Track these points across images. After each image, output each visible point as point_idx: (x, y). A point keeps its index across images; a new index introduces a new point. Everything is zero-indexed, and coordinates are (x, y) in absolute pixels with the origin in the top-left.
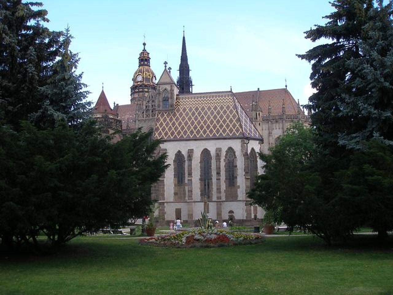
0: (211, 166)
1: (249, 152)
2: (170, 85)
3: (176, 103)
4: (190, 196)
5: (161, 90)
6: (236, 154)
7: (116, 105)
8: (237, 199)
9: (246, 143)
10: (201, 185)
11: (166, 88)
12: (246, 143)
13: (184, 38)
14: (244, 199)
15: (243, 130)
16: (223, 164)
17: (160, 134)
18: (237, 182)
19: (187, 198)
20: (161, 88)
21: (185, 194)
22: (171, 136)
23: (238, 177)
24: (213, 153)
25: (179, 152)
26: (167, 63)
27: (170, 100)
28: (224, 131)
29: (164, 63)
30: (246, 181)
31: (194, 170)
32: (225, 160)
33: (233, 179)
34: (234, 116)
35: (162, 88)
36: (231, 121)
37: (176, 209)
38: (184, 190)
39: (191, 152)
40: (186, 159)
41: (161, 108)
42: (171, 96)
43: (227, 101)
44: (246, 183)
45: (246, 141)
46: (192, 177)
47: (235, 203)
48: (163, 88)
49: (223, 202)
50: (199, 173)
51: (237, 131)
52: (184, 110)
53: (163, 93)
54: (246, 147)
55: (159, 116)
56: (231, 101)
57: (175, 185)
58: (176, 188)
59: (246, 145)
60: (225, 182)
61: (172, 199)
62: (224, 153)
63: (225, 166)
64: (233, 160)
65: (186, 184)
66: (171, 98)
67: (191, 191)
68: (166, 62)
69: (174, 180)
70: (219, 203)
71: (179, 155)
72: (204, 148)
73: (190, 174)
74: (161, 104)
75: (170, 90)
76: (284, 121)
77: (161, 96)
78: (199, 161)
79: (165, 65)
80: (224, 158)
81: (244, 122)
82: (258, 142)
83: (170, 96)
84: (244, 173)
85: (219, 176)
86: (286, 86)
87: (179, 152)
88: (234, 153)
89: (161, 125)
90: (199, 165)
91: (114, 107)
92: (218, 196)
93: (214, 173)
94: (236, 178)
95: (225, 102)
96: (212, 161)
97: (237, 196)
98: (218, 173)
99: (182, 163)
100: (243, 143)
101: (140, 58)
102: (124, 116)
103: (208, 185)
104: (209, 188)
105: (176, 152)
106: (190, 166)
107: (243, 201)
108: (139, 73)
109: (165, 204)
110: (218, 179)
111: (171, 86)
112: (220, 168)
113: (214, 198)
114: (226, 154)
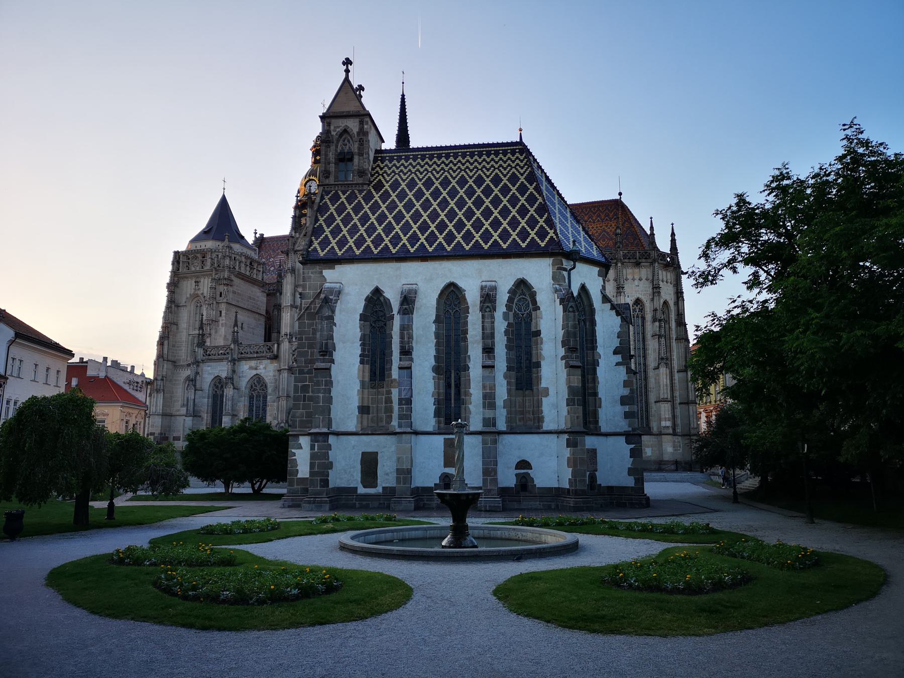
0: (466, 332)
1: (575, 291)
2: (357, 120)
3: (373, 169)
4: (406, 416)
5: (334, 133)
6: (539, 298)
7: (258, 236)
8: (540, 427)
9: (565, 270)
10: (437, 386)
11: (346, 126)
12: (565, 270)
13: (403, 96)
14: (563, 426)
15: (558, 232)
16: (501, 326)
17: (325, 243)
18: (539, 379)
19: (395, 423)
20: (332, 128)
21: (389, 410)
22: (354, 248)
23: (543, 363)
24: (473, 297)
25: (377, 292)
26: (351, 63)
27: (356, 159)
28: (505, 235)
29: (344, 63)
30: (568, 375)
31: (416, 344)
32: (505, 316)
33: (529, 371)
34: (531, 200)
35: (335, 127)
36: (523, 212)
37: (363, 453)
38: (389, 400)
39: (408, 301)
40: (395, 311)
41: (331, 180)
42: (359, 149)
43: (509, 165)
44: (568, 381)
45: (567, 264)
46: (412, 360)
47: (535, 438)
48: (339, 127)
49: (500, 433)
50: (433, 352)
51: (542, 234)
52: (395, 185)
53: (338, 141)
54: (567, 280)
55: (326, 199)
56: (522, 164)
57: (363, 384)
58: (366, 391)
59: (565, 274)
60: (505, 377)
61: (352, 424)
62: (502, 298)
63: (506, 332)
64: (530, 315)
65: (395, 380)
66: (361, 154)
67: (407, 402)
68: (347, 59)
69: (359, 370)
70: (489, 438)
71: (376, 301)
72: (448, 281)
73: (406, 352)
74: (332, 168)
75: (358, 133)
76: (619, 265)
77: (333, 147)
78: (434, 318)
79: (345, 67)
80: (505, 310)
81: (558, 215)
82: (596, 270)
83: (355, 148)
84: (562, 352)
85: (490, 358)
86: (620, 194)
87: (377, 292)
88: (533, 295)
89: (330, 220)
90: (433, 328)
91: (253, 239)
92: (487, 416)
93: (475, 353)
94: (538, 365)
95: (505, 166)
96: (471, 319)
97: (540, 420)
98: (488, 350)
99: (385, 325)
100: (559, 269)
101: (314, 146)
102: (273, 258)
103: (458, 386)
104: (458, 393)
105: (368, 291)
106: (406, 329)
107: (559, 433)
108: (311, 178)
109: (332, 439)
110: (488, 367)
111: (361, 123)
112: (492, 335)
113: (475, 423)
114: (510, 300)
